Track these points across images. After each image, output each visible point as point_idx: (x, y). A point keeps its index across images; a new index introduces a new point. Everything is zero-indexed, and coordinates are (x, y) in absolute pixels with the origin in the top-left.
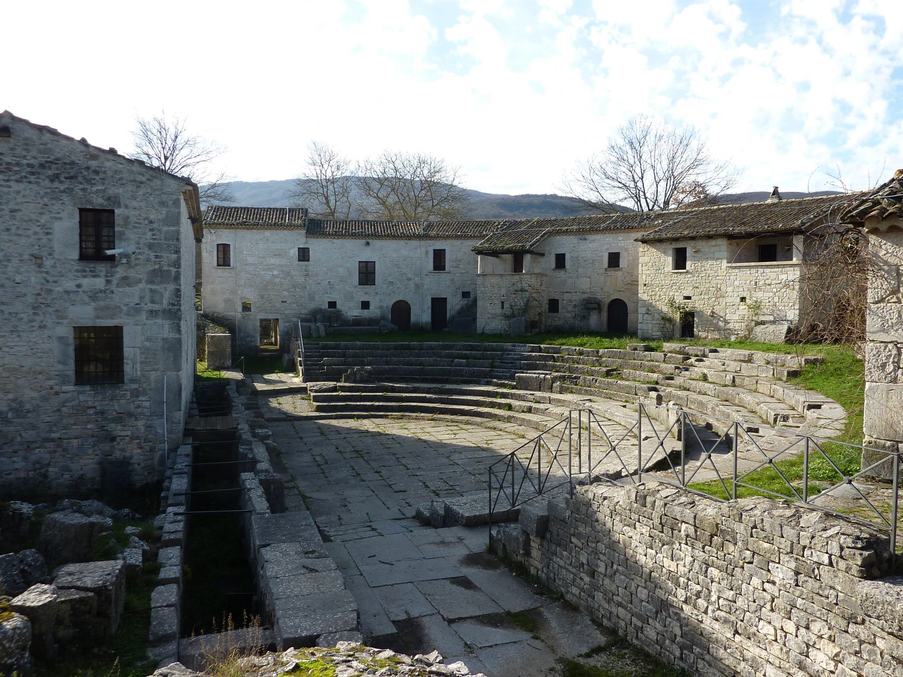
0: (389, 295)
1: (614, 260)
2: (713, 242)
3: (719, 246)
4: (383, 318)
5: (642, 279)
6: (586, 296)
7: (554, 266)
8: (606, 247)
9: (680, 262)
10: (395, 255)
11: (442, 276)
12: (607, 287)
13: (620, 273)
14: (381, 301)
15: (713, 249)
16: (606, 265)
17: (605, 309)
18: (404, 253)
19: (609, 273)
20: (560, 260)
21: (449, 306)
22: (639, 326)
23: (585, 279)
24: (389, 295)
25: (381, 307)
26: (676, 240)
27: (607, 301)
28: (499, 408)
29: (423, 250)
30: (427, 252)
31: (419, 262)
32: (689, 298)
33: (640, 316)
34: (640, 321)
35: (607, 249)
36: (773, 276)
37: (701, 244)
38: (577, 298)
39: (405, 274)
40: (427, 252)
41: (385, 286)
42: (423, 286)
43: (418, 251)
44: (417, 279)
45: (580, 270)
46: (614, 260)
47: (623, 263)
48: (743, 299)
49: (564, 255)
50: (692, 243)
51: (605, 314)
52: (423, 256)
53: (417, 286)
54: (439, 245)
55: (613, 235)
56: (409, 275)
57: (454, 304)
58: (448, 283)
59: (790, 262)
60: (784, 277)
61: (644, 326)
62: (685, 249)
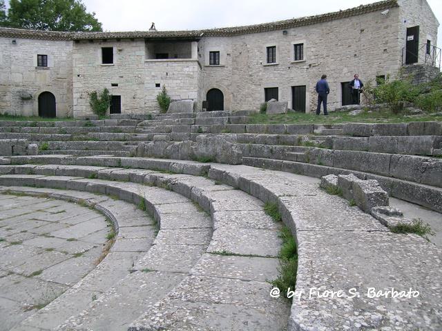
1: (43, 61)
2: (134, 44)
3: (140, 46)
5: (76, 71)
8: (35, 49)
9: (108, 57)
12: (41, 82)
16: (36, 65)
17: (37, 100)
19: (39, 71)
22: (75, 108)
26: (105, 40)
32: (117, 85)
33: (75, 100)
34: (75, 104)
36: (179, 68)
37: (124, 46)
45: (13, 67)
46: (43, 61)
47: (50, 63)
48: (158, 85)
50: (118, 44)
55: (41, 41)
59: (191, 60)
61: (79, 108)
62: (112, 48)
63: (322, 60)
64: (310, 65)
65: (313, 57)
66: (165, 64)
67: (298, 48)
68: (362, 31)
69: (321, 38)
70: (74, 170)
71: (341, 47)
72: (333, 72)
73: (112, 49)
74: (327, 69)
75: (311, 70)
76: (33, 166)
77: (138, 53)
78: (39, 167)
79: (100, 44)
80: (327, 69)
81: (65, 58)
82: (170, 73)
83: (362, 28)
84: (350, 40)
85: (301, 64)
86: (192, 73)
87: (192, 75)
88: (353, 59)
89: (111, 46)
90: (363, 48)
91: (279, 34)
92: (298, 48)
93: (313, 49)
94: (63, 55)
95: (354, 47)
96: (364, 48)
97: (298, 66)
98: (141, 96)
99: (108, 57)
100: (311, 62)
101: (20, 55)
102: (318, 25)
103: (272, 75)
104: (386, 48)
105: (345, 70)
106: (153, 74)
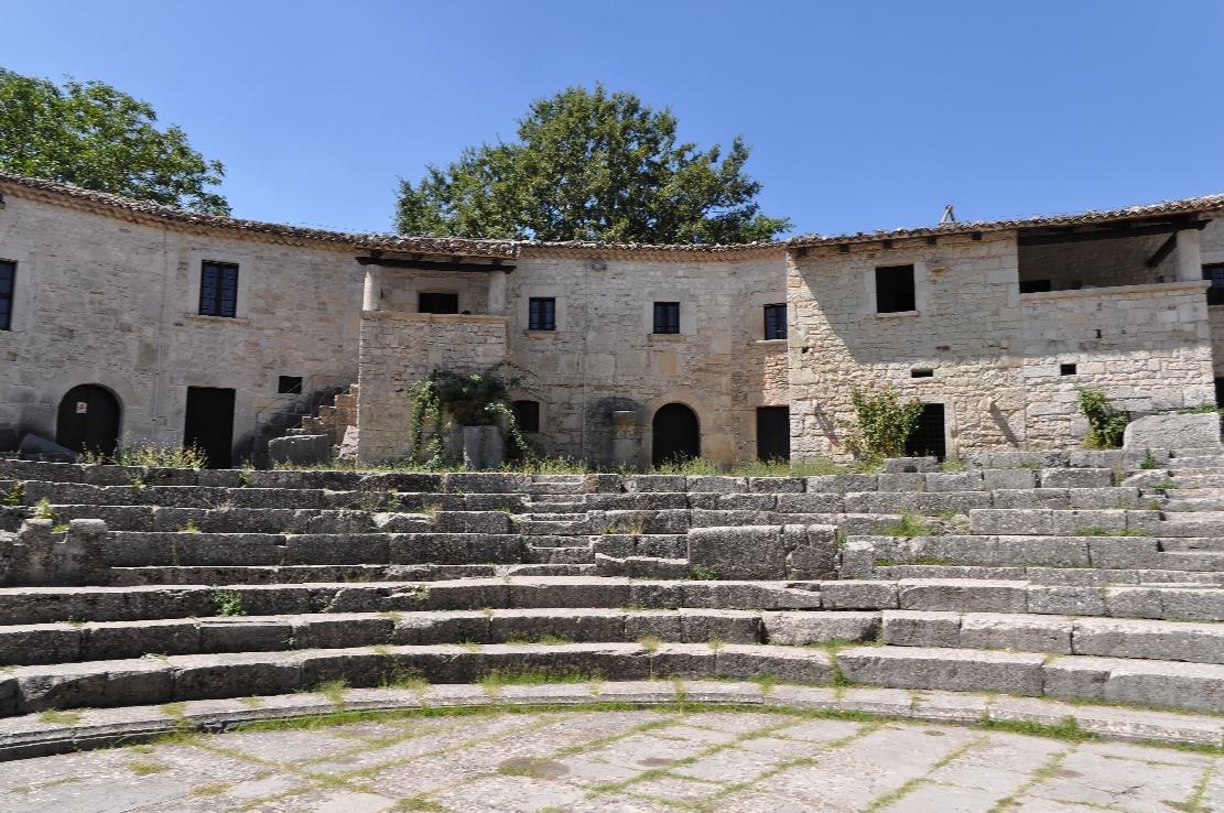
0: (58, 364)
1: (667, 318)
2: (982, 250)
4: (26, 429)
6: (605, 394)
7: (526, 324)
8: (647, 290)
10: (85, 255)
11: (227, 328)
13: (680, 347)
14: (25, 379)
15: (983, 265)
16: (650, 328)
18: (117, 254)
19: (658, 346)
20: (542, 313)
21: (239, 410)
23: (601, 357)
24: (58, 364)
25: (26, 398)
26: (887, 243)
27: (656, 405)
28: (391, 681)
29: (173, 257)
30: (183, 266)
31: (157, 287)
35: (650, 294)
38: (580, 398)
39: (115, 312)
40: (183, 266)
41: (45, 338)
42: (166, 353)
43: (159, 257)
44: (149, 332)
45: (591, 336)
46: (667, 318)
47: (687, 323)
48: (1068, 370)
49: (552, 300)
50: (929, 252)
51: (648, 436)
52: (172, 272)
53: (149, 352)
54: (222, 251)
56: (126, 318)
57: (255, 405)
58: (241, 350)
60: (1171, 316)
62: (910, 268)
66: (1091, 304)
70: (1149, 636)
73: (908, 270)
76: (952, 617)
77: (995, 277)
78: (973, 621)
79: (872, 256)
81: (725, 310)
82: (1110, 333)
86: (1189, 328)
87: (1193, 333)
89: (903, 262)
94: (722, 300)
98: (1015, 404)
99: (896, 291)
101: (609, 304)
106: (1051, 335)
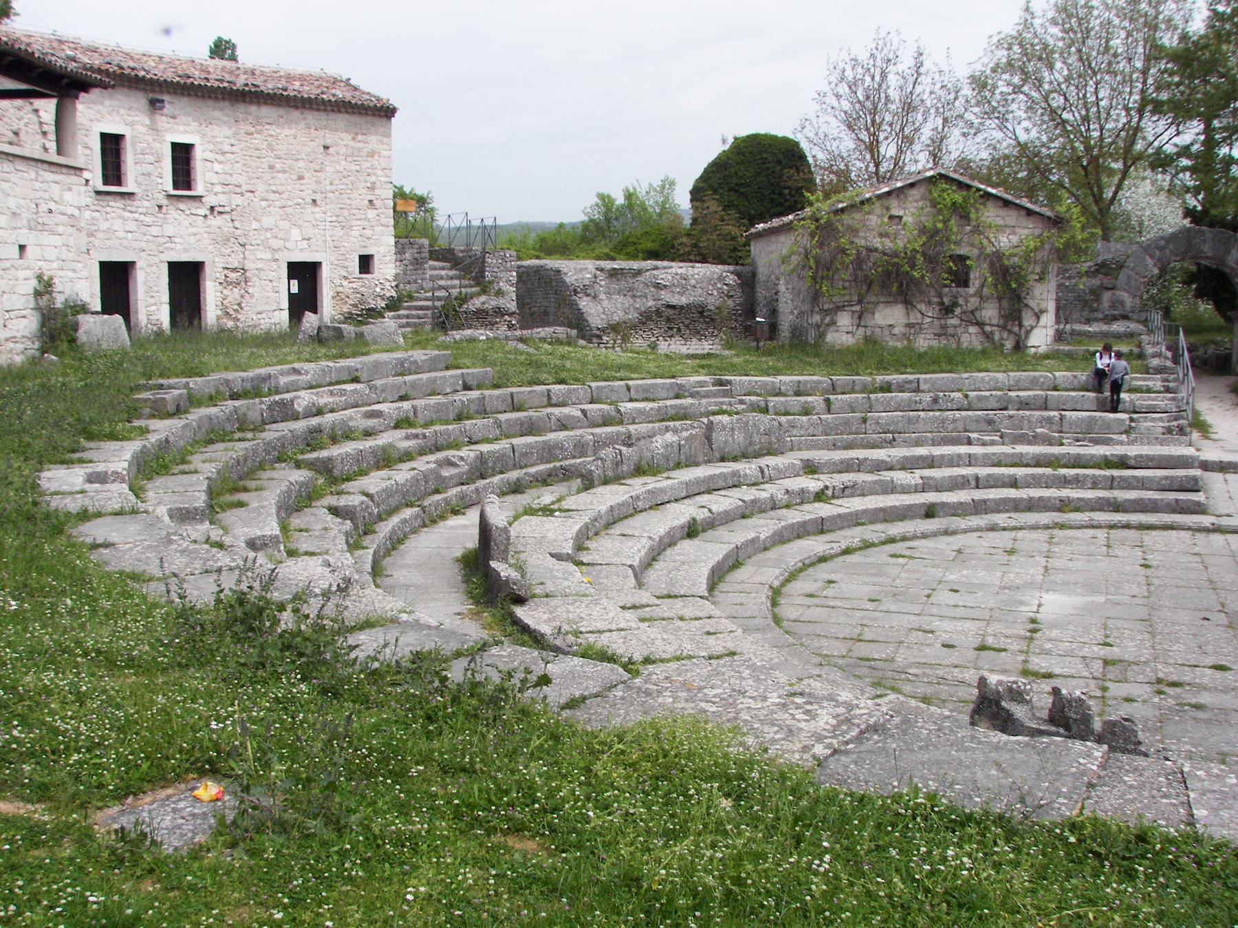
63: (238, 200)
64: (212, 208)
65: (218, 188)
67: (182, 155)
68: (326, 148)
69: (233, 142)
71: (280, 175)
72: (269, 235)
74: (255, 225)
75: (216, 221)
80: (255, 225)
83: (328, 142)
84: (301, 164)
85: (191, 204)
88: (310, 209)
90: (328, 188)
91: (139, 100)
92: (182, 155)
93: (217, 167)
95: (310, 182)
96: (333, 188)
97: (182, 206)
100: (210, 200)
102: (227, 104)
103: (118, 225)
104: (372, 198)
105: (296, 234)
